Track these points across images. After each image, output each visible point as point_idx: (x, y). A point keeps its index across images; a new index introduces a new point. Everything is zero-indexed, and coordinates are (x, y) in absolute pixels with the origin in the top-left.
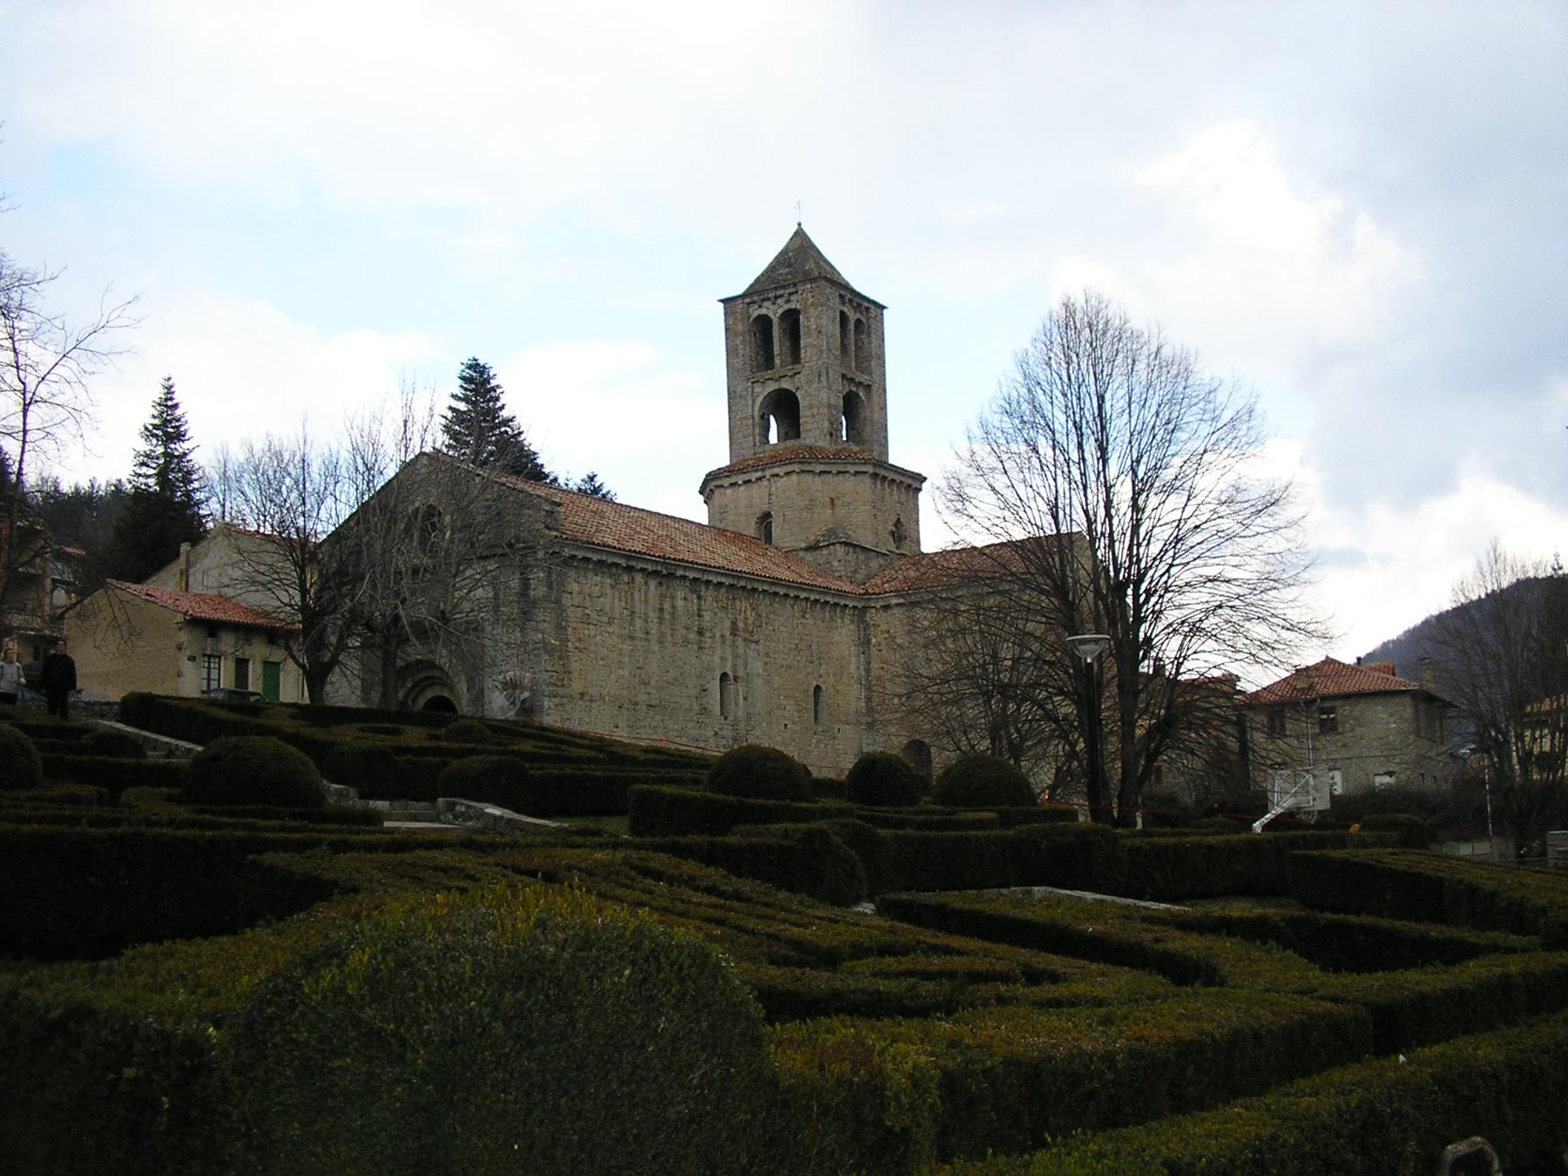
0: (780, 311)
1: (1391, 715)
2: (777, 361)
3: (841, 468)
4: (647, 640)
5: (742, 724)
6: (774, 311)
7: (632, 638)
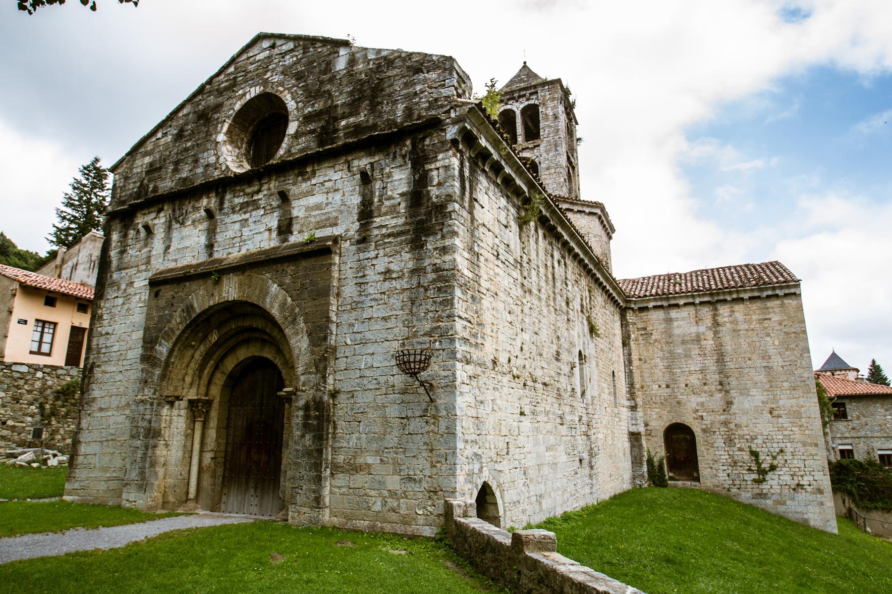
0: (522, 106)
1: (886, 410)
2: (520, 139)
3: (580, 209)
4: (540, 299)
5: (590, 407)
6: (517, 107)
7: (530, 291)
